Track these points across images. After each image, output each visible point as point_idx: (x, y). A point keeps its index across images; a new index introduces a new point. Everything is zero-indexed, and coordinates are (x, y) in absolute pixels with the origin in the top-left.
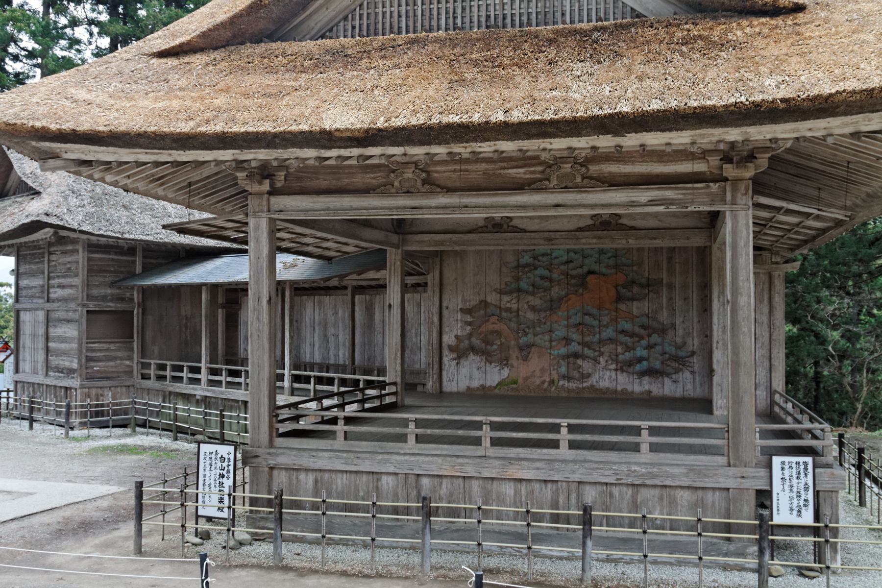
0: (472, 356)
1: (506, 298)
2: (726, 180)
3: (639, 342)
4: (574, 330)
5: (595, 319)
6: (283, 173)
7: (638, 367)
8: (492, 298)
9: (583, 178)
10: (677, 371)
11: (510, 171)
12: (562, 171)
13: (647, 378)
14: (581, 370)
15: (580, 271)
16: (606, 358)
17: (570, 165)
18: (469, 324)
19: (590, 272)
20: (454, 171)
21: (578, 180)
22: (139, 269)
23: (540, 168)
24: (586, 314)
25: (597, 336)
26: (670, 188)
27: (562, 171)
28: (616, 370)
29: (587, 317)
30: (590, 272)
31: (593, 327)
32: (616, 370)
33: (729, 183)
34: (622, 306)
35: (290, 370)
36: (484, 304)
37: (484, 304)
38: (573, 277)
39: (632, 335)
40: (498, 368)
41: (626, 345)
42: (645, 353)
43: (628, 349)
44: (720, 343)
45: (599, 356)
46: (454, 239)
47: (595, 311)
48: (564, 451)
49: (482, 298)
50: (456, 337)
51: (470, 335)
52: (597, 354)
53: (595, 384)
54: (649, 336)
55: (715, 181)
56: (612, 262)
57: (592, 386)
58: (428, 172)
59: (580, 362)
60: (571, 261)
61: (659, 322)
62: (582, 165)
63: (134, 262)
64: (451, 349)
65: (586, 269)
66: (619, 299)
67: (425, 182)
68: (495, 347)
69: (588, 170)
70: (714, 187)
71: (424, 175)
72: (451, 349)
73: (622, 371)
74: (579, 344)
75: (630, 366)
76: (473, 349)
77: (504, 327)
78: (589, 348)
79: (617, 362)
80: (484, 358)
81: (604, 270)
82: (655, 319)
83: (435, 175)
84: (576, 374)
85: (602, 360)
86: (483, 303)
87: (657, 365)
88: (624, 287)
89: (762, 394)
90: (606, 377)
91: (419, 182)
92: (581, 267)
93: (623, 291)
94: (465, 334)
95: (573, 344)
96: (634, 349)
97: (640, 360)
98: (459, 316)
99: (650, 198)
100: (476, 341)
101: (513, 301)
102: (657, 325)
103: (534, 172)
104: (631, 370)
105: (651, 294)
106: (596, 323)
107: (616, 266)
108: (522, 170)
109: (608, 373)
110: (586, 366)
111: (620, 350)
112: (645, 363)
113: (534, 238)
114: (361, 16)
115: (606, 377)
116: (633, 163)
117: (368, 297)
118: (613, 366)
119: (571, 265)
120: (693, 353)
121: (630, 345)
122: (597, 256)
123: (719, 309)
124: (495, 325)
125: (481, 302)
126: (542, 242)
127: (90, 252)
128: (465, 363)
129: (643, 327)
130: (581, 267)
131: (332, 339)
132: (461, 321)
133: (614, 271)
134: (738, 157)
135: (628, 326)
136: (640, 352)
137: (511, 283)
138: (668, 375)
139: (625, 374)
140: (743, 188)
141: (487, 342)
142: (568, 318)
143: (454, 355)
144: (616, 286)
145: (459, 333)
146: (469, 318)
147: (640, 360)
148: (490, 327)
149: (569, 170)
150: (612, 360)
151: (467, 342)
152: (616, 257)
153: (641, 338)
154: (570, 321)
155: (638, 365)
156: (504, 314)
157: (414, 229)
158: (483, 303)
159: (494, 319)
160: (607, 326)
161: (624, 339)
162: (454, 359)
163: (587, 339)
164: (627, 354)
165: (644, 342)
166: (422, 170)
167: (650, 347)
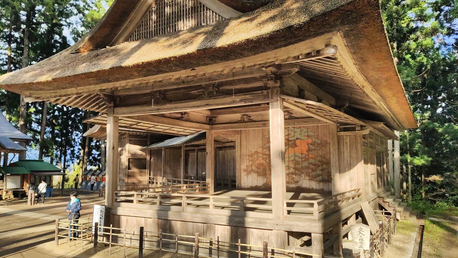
0: (253, 174)
1: (265, 150)
2: (269, 88)
3: (318, 167)
4: (291, 163)
5: (299, 158)
6: (119, 99)
7: (318, 178)
9: (217, 92)
11: (192, 92)
12: (209, 90)
13: (322, 183)
14: (295, 180)
15: (293, 138)
16: (305, 175)
17: (212, 88)
18: (252, 161)
19: (297, 139)
20: (174, 93)
21: (215, 93)
22: (148, 143)
23: (202, 90)
24: (296, 156)
25: (301, 165)
26: (248, 94)
27: (209, 90)
28: (309, 180)
29: (296, 157)
30: (297, 139)
31: (299, 162)
32: (309, 180)
33: (270, 91)
35: (183, 179)
38: (291, 141)
40: (262, 178)
41: (313, 169)
42: (321, 172)
44: (334, 167)
45: (302, 174)
46: (229, 126)
47: (300, 155)
49: (256, 150)
50: (247, 166)
51: (252, 165)
52: (301, 173)
53: (300, 185)
54: (322, 165)
55: (265, 90)
56: (306, 134)
57: (299, 186)
58: (164, 95)
60: (290, 134)
61: (326, 159)
62: (216, 87)
63: (147, 141)
64: (244, 170)
65: (295, 138)
67: (163, 98)
68: (261, 170)
69: (219, 89)
70: (265, 92)
71: (163, 96)
72: (244, 170)
74: (293, 168)
75: (314, 178)
77: (264, 162)
78: (298, 170)
79: (309, 176)
80: (257, 174)
81: (303, 138)
82: (324, 158)
83: (168, 96)
86: (256, 153)
88: (311, 144)
90: (305, 183)
91: (161, 99)
92: (294, 136)
93: (311, 146)
94: (249, 164)
95: (291, 168)
96: (316, 171)
99: (241, 99)
100: (254, 168)
101: (267, 151)
102: (325, 161)
103: (199, 92)
104: (315, 179)
105: (323, 147)
106: (300, 160)
107: (308, 136)
108: (196, 91)
109: (306, 180)
111: (310, 171)
112: (321, 177)
113: (259, 124)
114: (135, 35)
115: (305, 183)
116: (235, 85)
117: (223, 151)
118: (308, 178)
119: (290, 136)
121: (314, 169)
122: (300, 132)
123: (333, 152)
124: (261, 161)
125: (255, 152)
126: (261, 126)
128: (250, 176)
130: (294, 136)
132: (248, 159)
133: (307, 138)
134: (270, 78)
137: (266, 144)
139: (312, 181)
140: (276, 91)
142: (289, 158)
143: (245, 173)
144: (308, 145)
146: (251, 158)
148: (259, 162)
149: (212, 90)
150: (307, 175)
151: (250, 168)
152: (308, 132)
153: (319, 166)
154: (290, 159)
155: (318, 178)
156: (264, 156)
157: (216, 123)
158: (256, 153)
159: (260, 159)
160: (304, 161)
162: (246, 175)
163: (297, 166)
164: (313, 173)
165: (320, 168)
166: (162, 94)
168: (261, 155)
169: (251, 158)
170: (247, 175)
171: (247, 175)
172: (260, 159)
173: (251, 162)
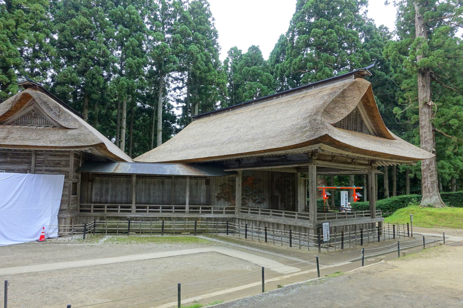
1: (230, 182)
8: (227, 182)
10: (264, 202)
15: (246, 176)
30: (248, 176)
34: (254, 185)
36: (225, 184)
37: (225, 184)
38: (245, 177)
39: (255, 193)
43: (255, 196)
48: (355, 218)
50: (218, 193)
51: (221, 193)
59: (245, 200)
66: (253, 183)
68: (227, 196)
73: (254, 202)
76: (222, 197)
78: (247, 196)
84: (245, 204)
85: (250, 199)
87: (260, 200)
89: (304, 206)
93: (254, 181)
97: (257, 199)
98: (219, 187)
100: (223, 195)
110: (247, 201)
111: (253, 197)
120: (266, 197)
127: (75, 157)
128: (220, 201)
129: (258, 191)
131: (152, 194)
135: (255, 190)
136: (257, 198)
138: (262, 203)
141: (225, 195)
145: (219, 192)
146: (221, 188)
147: (257, 199)
161: (254, 194)
163: (247, 194)
167: (259, 196)
168: (228, 186)
169: (221, 188)
170: (218, 200)
171: (218, 200)
172: (227, 188)
173: (221, 191)
